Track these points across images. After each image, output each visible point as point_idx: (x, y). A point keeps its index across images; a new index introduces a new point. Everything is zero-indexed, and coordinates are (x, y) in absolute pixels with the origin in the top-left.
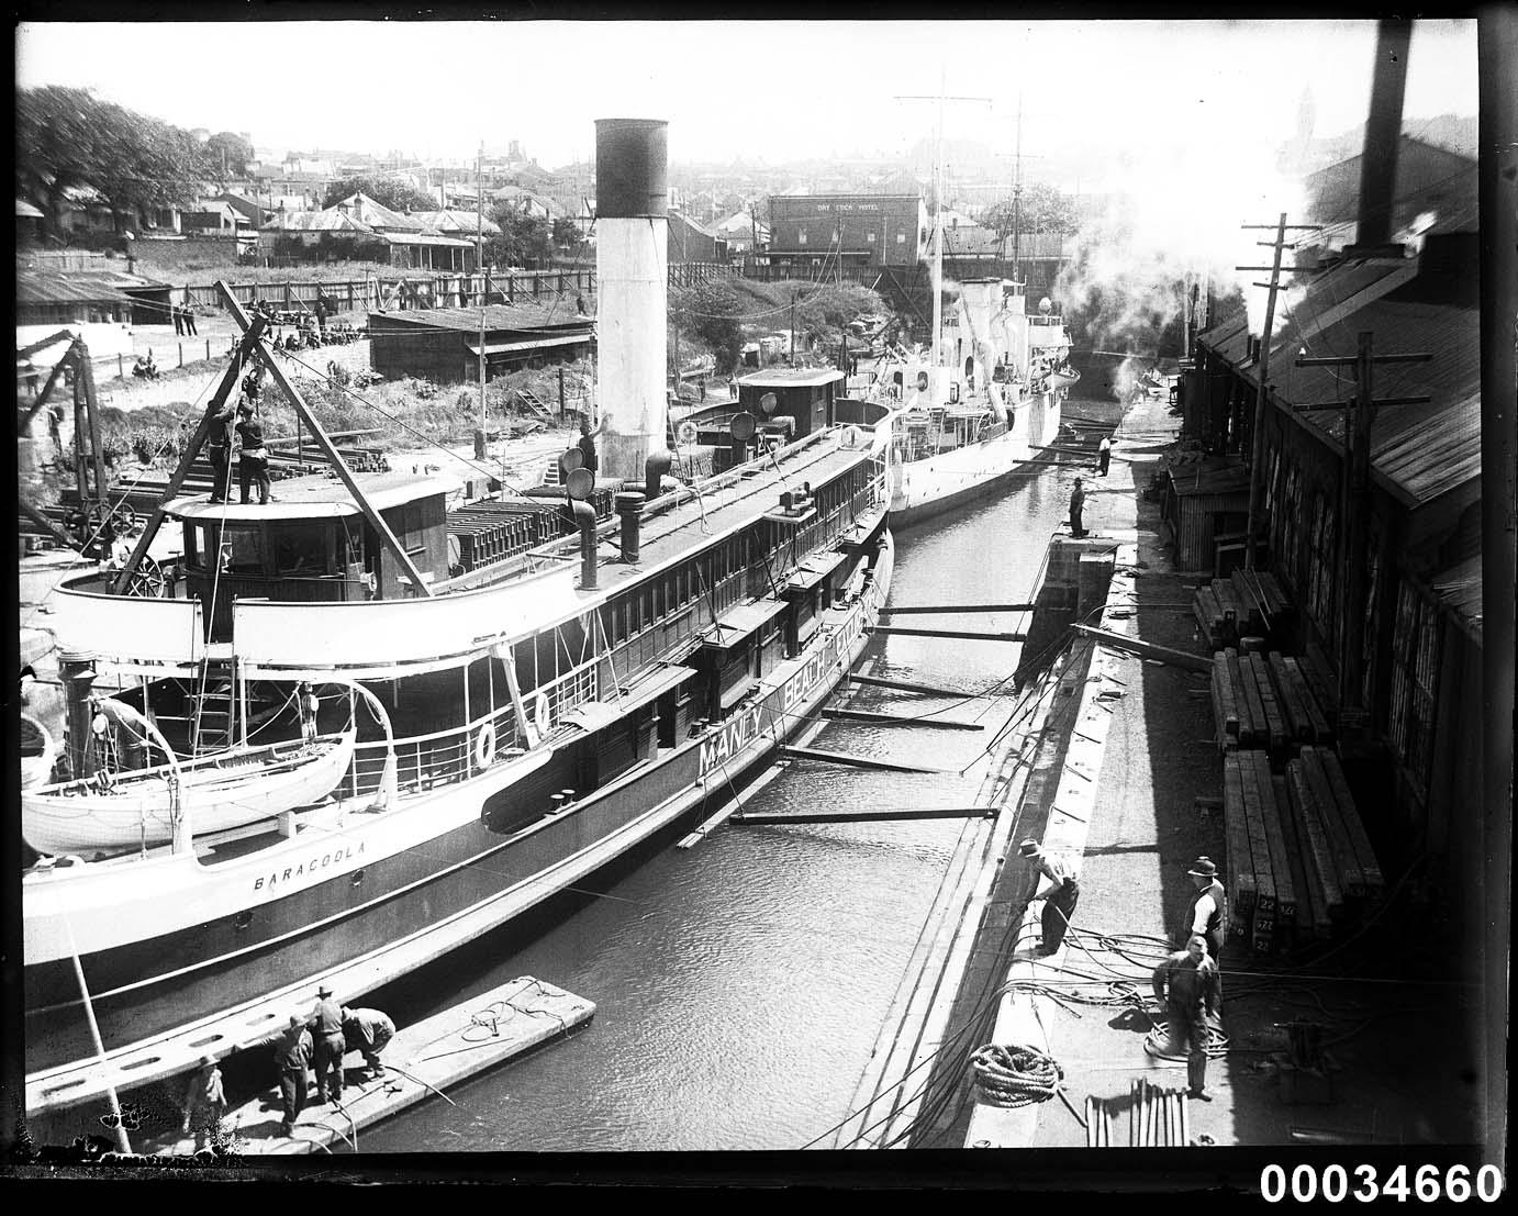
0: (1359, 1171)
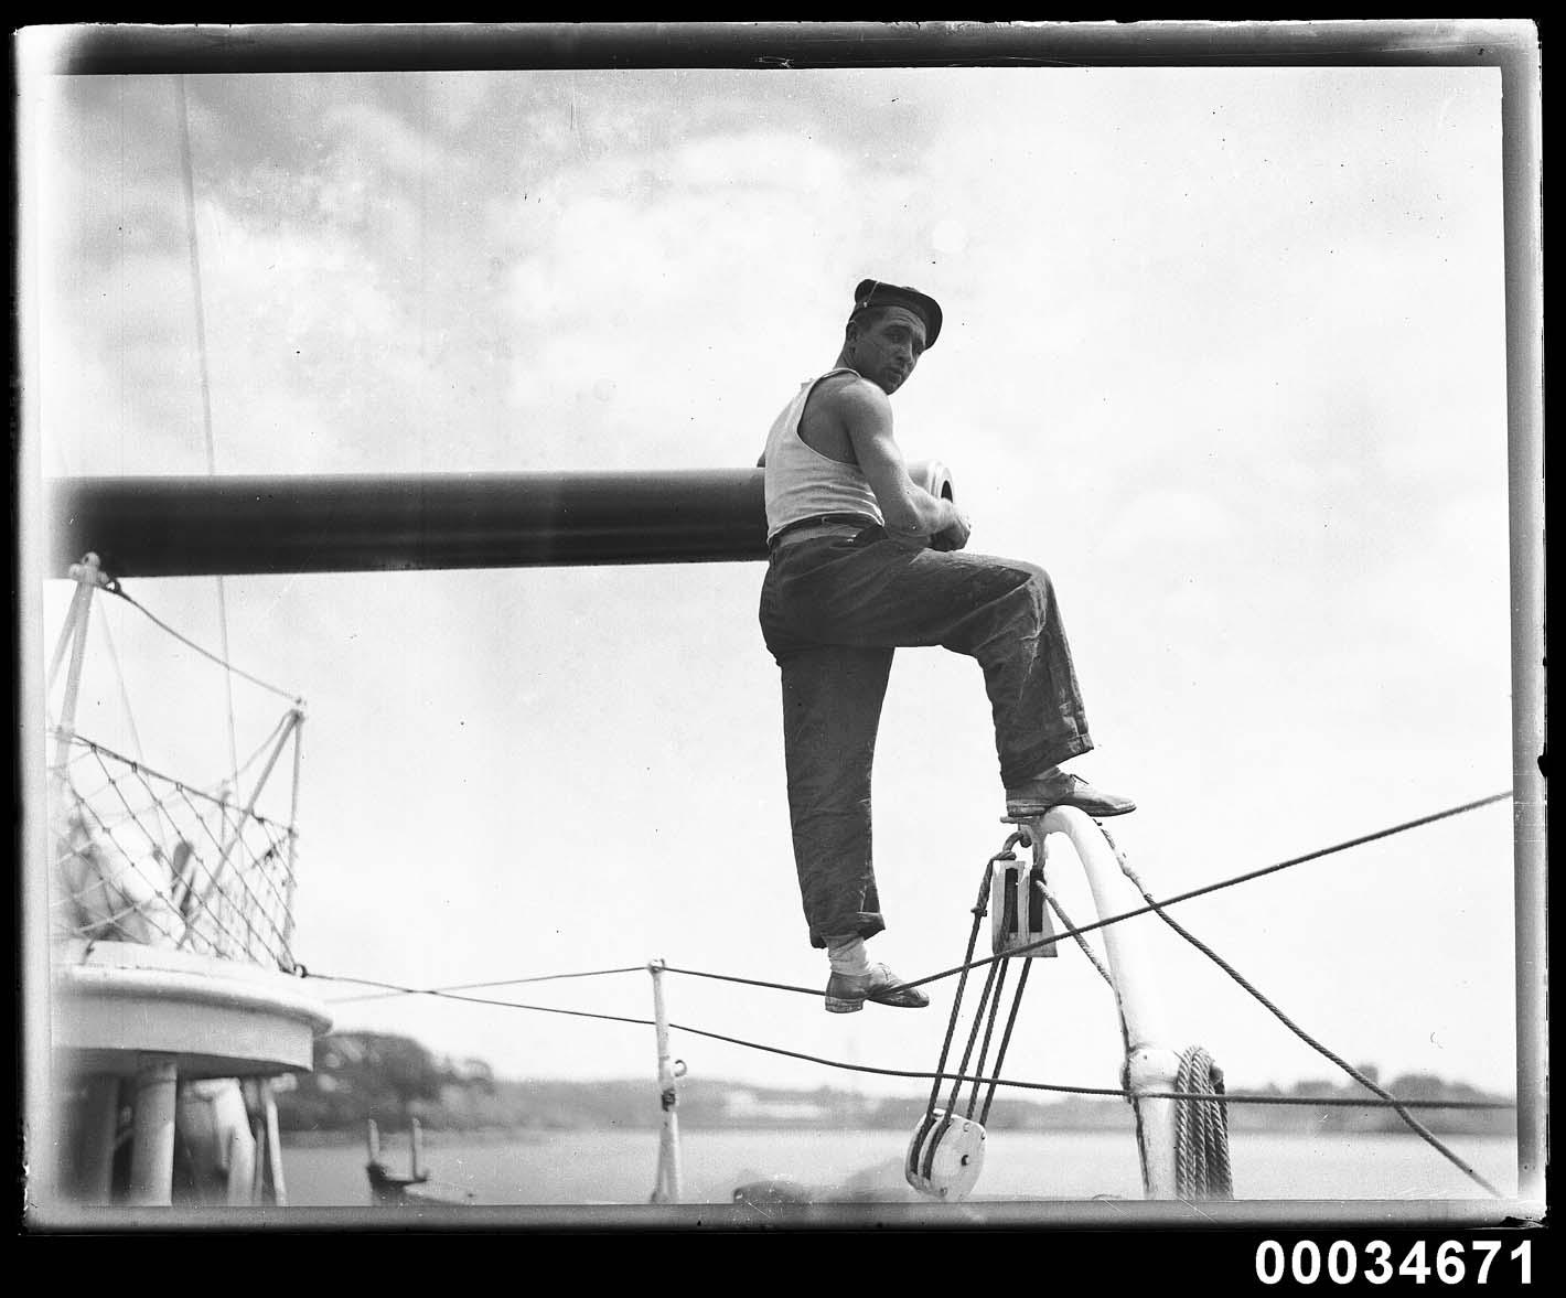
0: (1370, 1248)
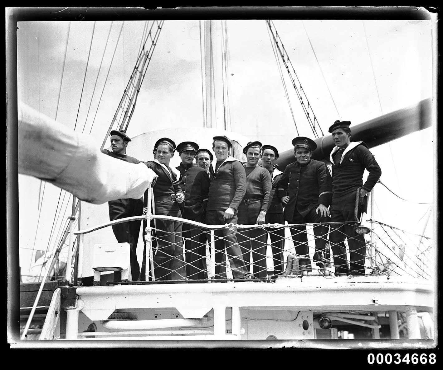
0: (395, 355)
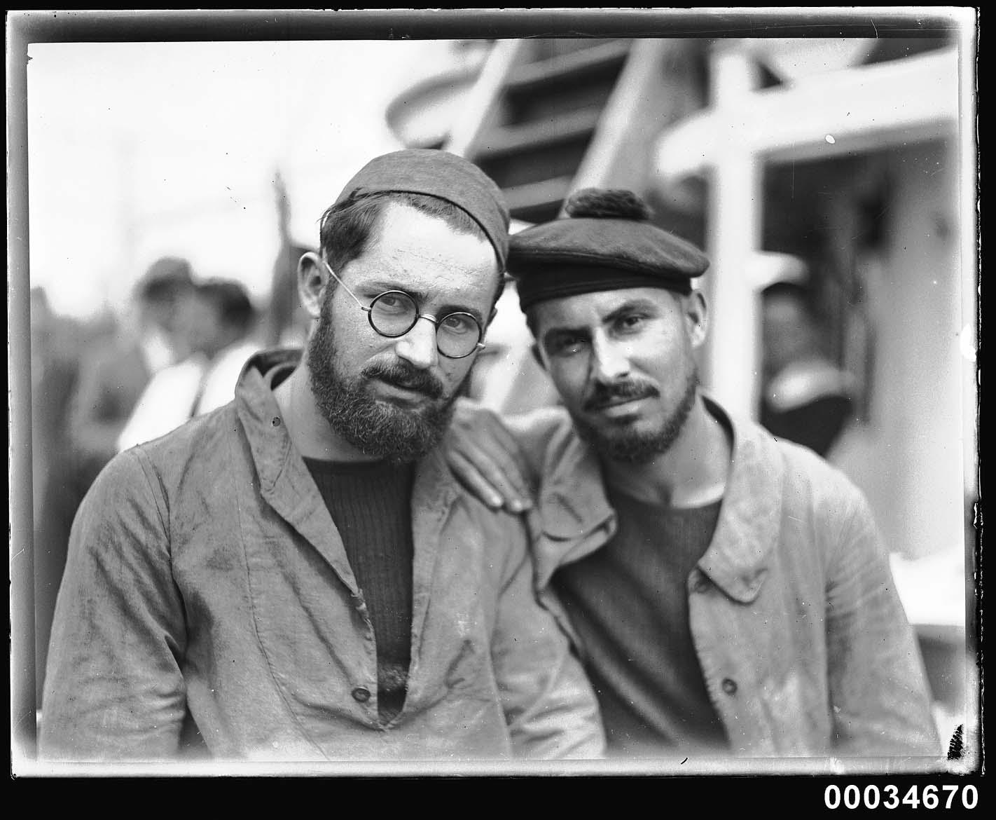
0: (887, 789)
